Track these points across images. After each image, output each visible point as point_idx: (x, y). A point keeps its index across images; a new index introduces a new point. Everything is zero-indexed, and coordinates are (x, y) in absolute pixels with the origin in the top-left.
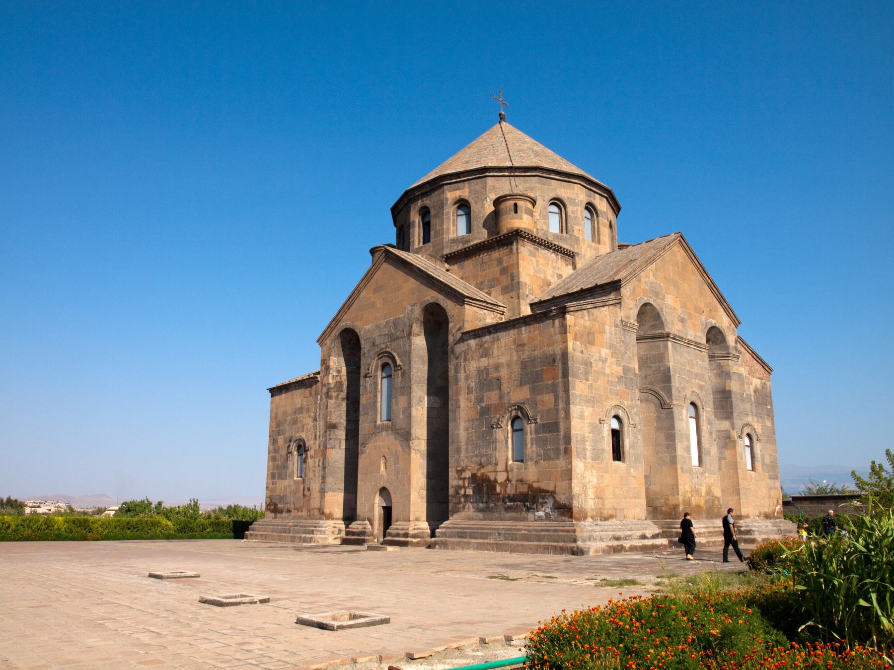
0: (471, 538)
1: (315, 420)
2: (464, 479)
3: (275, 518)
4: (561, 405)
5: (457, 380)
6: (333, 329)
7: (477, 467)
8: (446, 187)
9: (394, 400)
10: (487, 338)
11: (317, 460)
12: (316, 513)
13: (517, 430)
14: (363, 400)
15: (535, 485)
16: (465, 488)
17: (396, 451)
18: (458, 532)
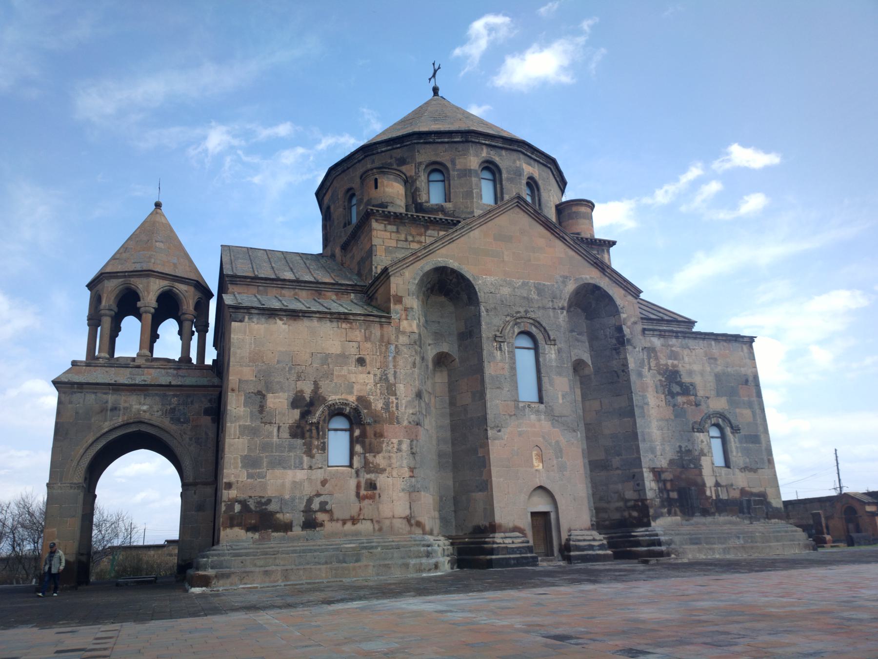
0: (707, 543)
1: (384, 378)
2: (665, 481)
3: (262, 539)
4: (759, 421)
5: (640, 375)
6: (418, 259)
7: (679, 470)
8: (522, 156)
9: (545, 380)
10: (673, 341)
11: (395, 441)
12: (400, 524)
13: (713, 437)
14: (490, 370)
15: (747, 489)
16: (668, 491)
17: (557, 442)
18: (690, 539)
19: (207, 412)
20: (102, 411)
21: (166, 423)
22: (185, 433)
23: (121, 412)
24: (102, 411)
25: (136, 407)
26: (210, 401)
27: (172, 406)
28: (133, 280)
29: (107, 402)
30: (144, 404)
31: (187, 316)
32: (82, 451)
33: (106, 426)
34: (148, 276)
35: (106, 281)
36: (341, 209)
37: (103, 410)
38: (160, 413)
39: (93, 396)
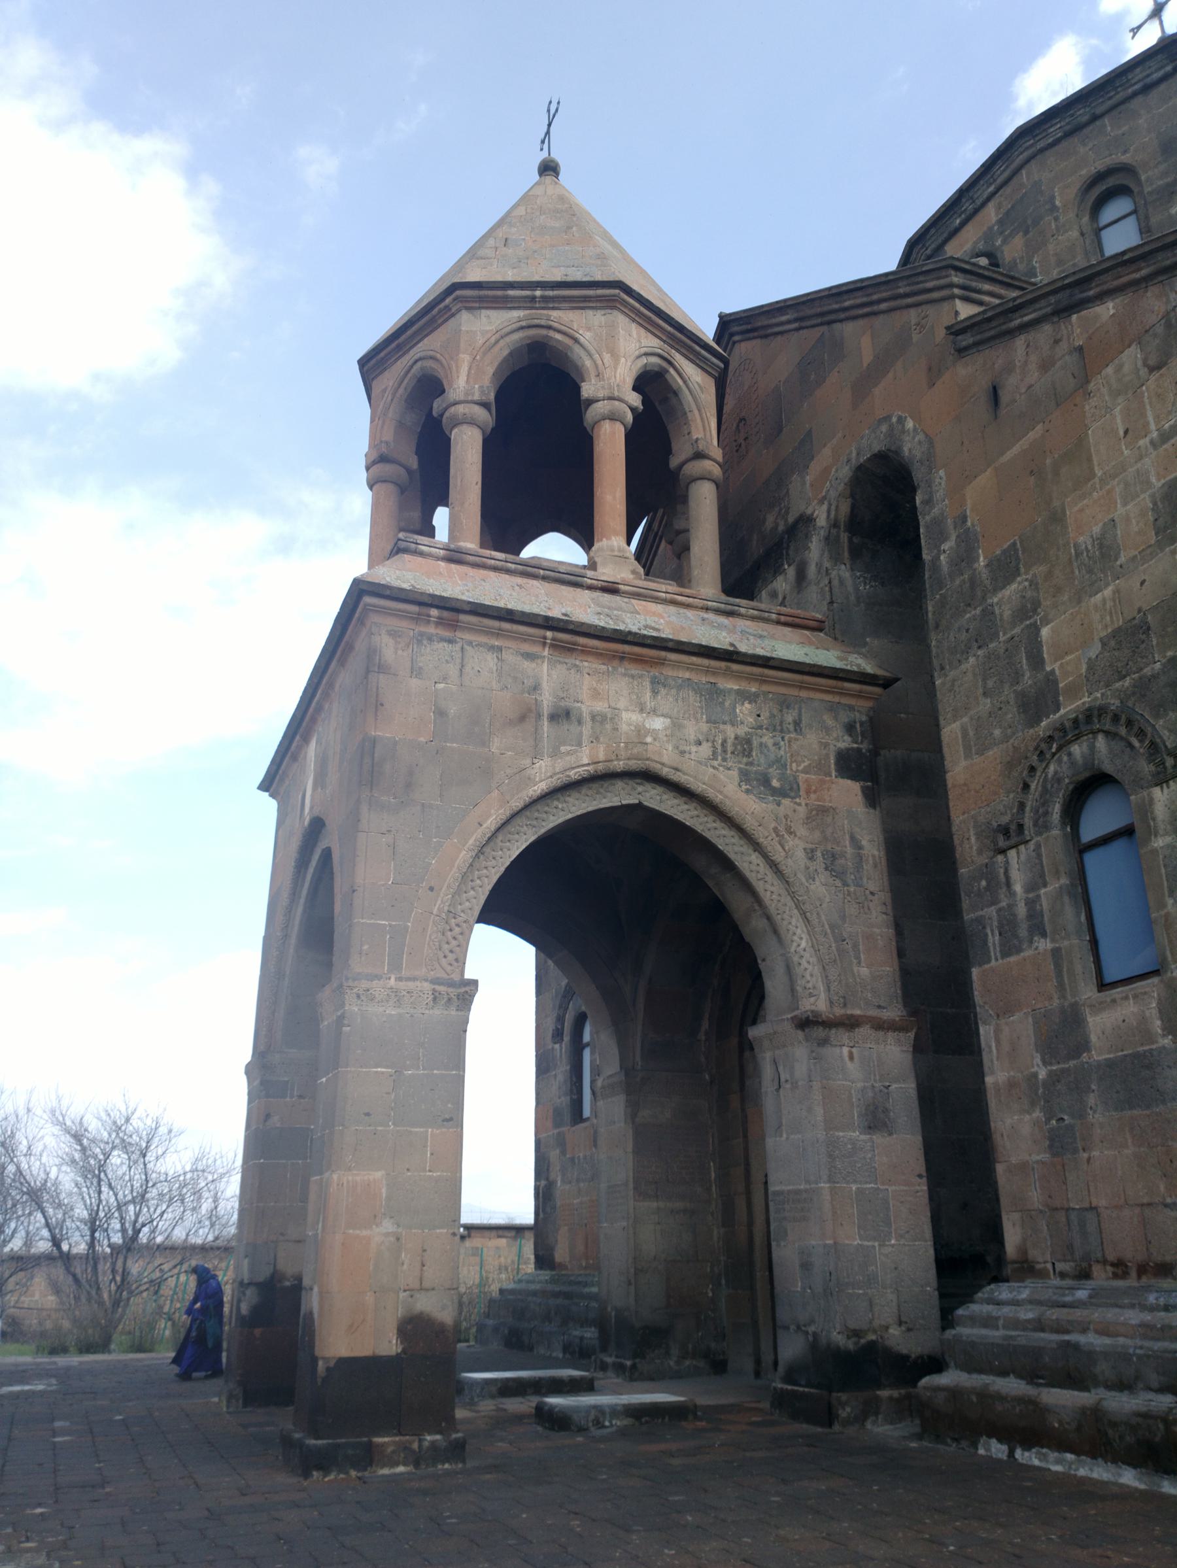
19: (849, 765)
20: (522, 718)
21: (726, 785)
22: (790, 832)
23: (586, 730)
24: (522, 718)
25: (630, 718)
26: (850, 728)
27: (742, 731)
28: (562, 317)
29: (536, 688)
30: (654, 712)
31: (708, 465)
32: (464, 856)
33: (543, 774)
34: (609, 304)
35: (465, 316)
36: (1075, 234)
37: (526, 715)
38: (705, 750)
39: (491, 660)
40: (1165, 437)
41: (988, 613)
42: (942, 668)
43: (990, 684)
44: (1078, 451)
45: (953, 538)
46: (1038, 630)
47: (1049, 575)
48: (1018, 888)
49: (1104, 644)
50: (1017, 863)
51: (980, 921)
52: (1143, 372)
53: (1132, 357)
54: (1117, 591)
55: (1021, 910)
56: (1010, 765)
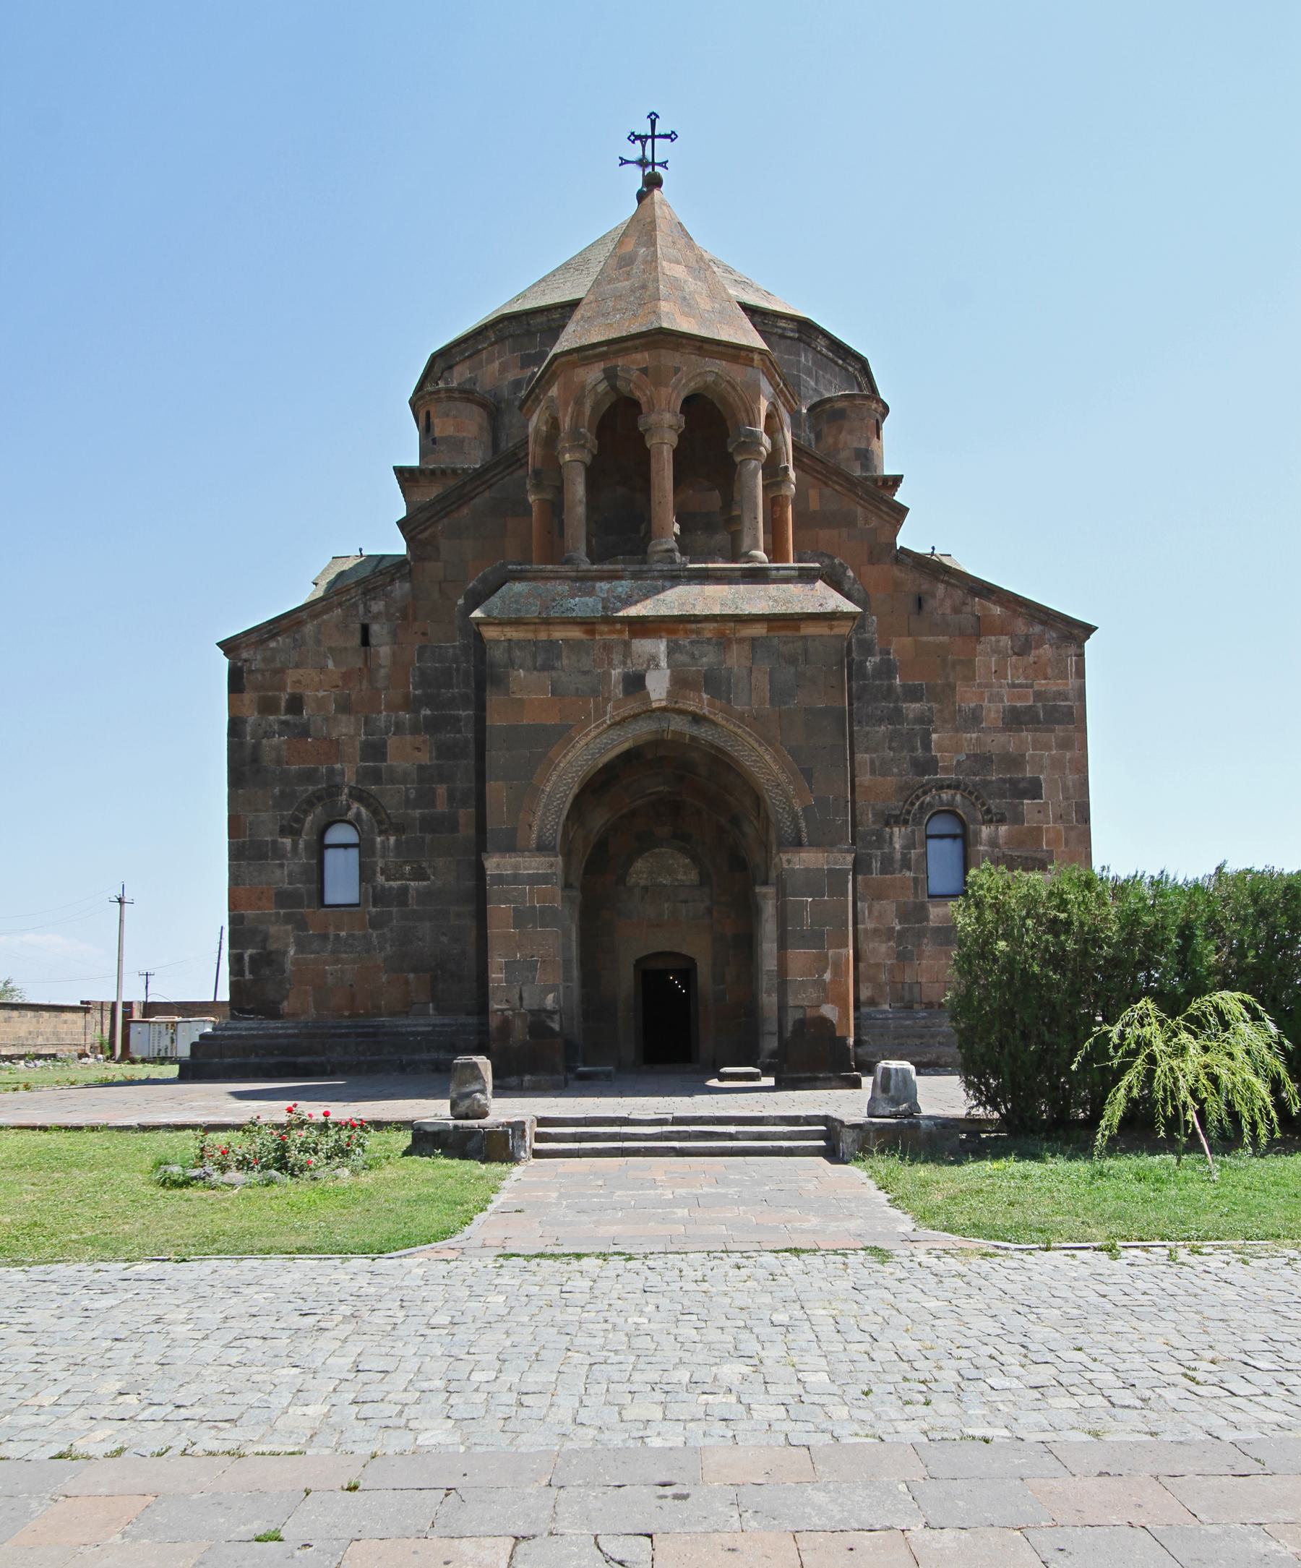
40: (1014, 686)
41: (898, 711)
42: (859, 722)
43: (894, 744)
44: (969, 663)
45: (878, 659)
46: (930, 734)
47: (941, 711)
48: (897, 846)
49: (968, 756)
50: (898, 836)
51: (868, 855)
52: (1010, 652)
53: (1005, 641)
54: (978, 739)
55: (898, 856)
56: (901, 789)
